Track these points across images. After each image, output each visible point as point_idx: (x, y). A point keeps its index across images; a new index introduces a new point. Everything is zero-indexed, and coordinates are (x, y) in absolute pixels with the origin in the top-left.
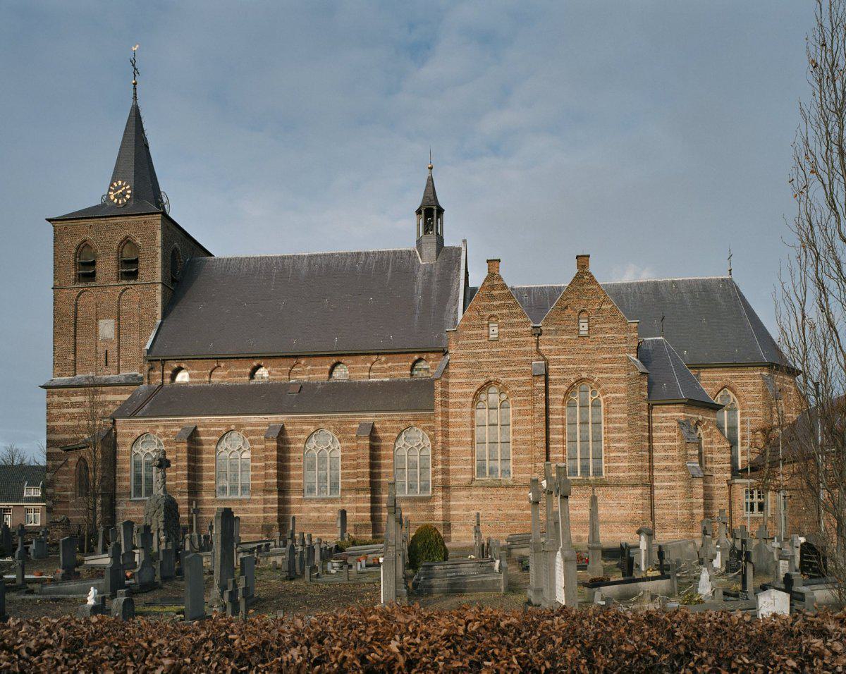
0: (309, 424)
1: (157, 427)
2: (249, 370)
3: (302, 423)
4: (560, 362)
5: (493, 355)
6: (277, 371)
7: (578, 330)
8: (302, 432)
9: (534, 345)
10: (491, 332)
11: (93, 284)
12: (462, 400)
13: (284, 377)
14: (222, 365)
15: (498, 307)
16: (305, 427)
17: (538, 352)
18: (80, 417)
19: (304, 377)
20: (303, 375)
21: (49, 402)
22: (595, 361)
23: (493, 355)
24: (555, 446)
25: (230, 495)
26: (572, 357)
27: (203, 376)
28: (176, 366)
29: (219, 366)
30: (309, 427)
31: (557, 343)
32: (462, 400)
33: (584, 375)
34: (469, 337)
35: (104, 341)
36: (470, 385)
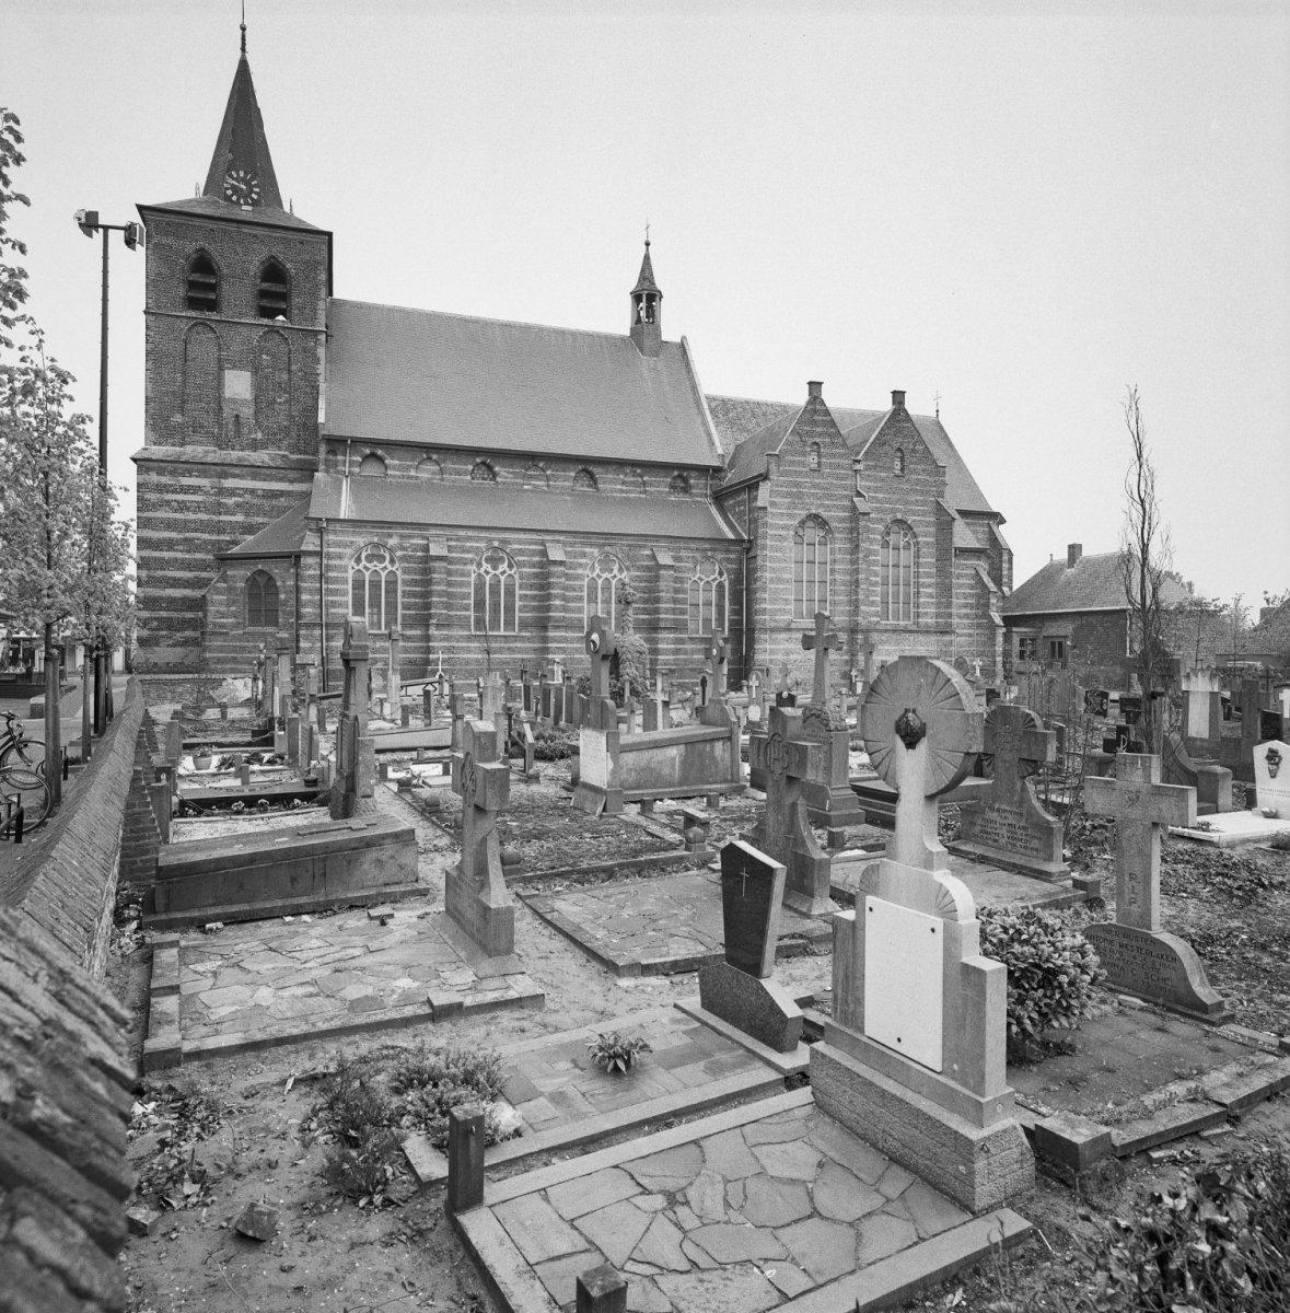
0: (591, 545)
1: (390, 536)
5: (815, 486)
8: (584, 555)
12: (783, 533)
14: (435, 457)
15: (820, 435)
16: (587, 550)
18: (198, 508)
21: (142, 481)
22: (907, 503)
23: (815, 486)
25: (520, 631)
27: (408, 468)
28: (368, 451)
31: (876, 479)
32: (783, 533)
33: (899, 516)
34: (792, 463)
35: (234, 401)
36: (791, 516)
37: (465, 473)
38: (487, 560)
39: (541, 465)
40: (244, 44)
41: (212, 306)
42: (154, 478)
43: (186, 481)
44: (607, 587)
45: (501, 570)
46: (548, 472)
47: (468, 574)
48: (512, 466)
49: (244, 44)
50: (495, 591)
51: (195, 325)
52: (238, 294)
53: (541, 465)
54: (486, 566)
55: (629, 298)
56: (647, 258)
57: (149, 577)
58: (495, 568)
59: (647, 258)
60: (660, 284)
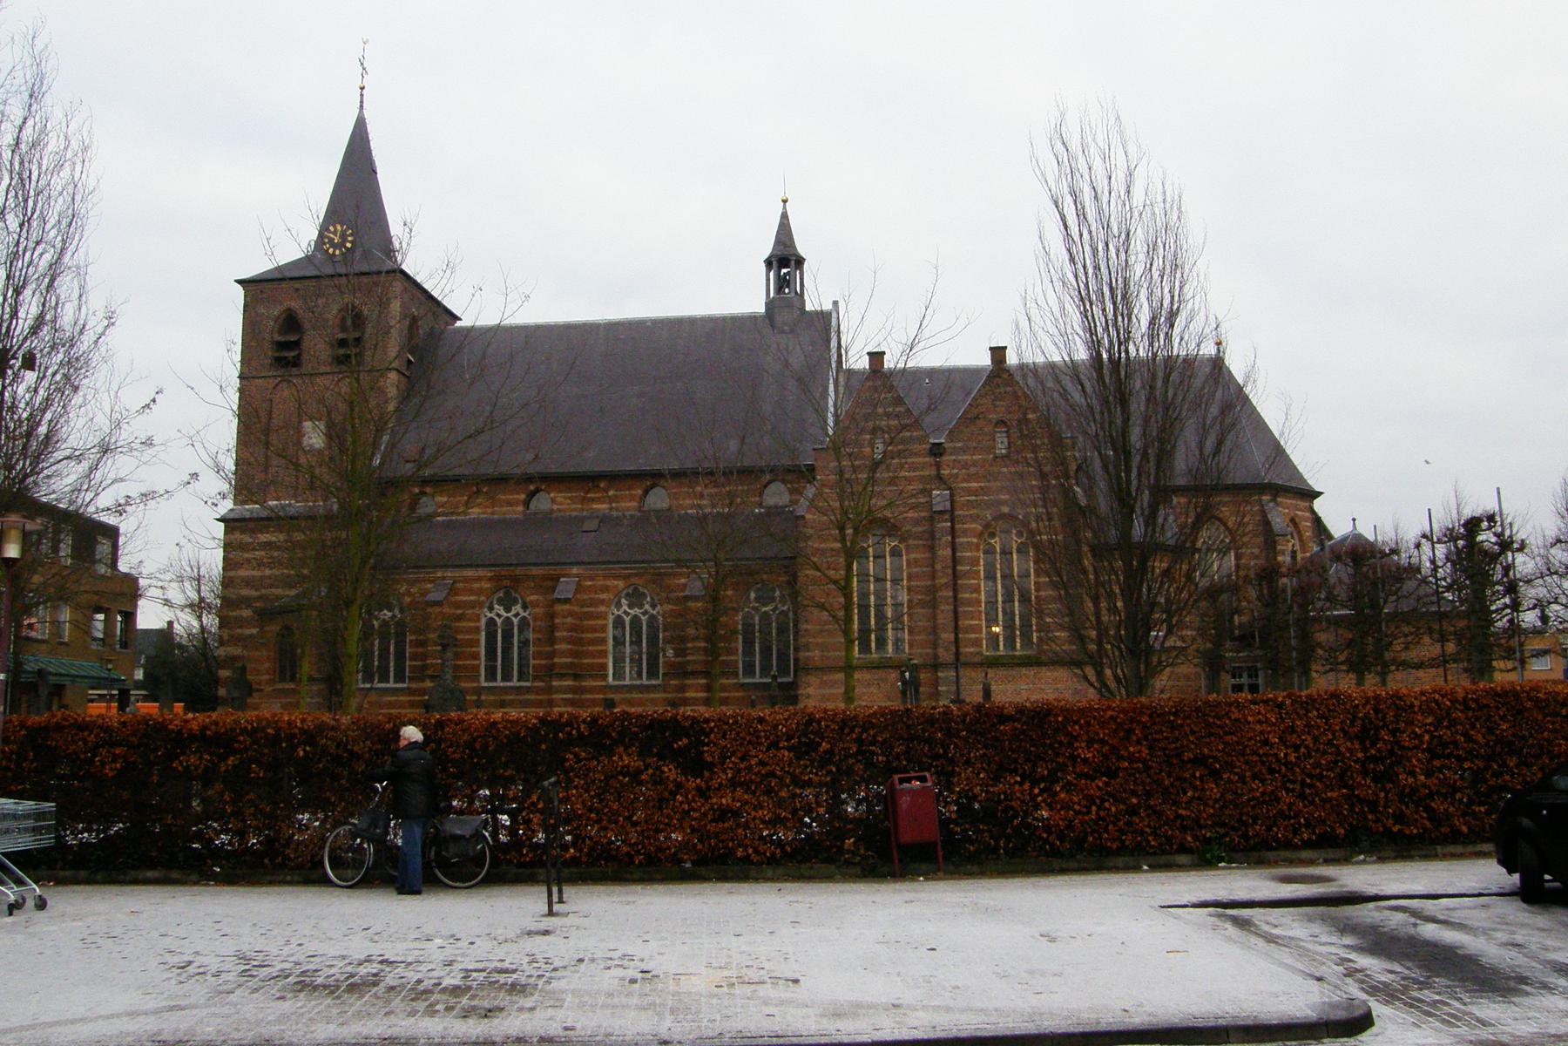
0: (617, 577)
2: (523, 497)
3: (606, 577)
4: (969, 491)
6: (564, 497)
7: (994, 448)
8: (606, 589)
9: (934, 468)
10: (876, 451)
11: (295, 371)
13: (574, 506)
16: (609, 583)
17: (939, 478)
19: (604, 506)
20: (602, 503)
24: (966, 609)
26: (987, 484)
29: (479, 491)
30: (616, 583)
33: (1006, 510)
37: (517, 504)
38: (500, 602)
39: (602, 485)
40: (362, 102)
41: (296, 362)
42: (238, 536)
43: (263, 538)
44: (636, 621)
45: (513, 612)
46: (611, 493)
47: (603, 616)
48: (570, 490)
49: (362, 102)
50: (508, 635)
51: (280, 382)
52: (317, 346)
53: (602, 485)
54: (499, 609)
55: (764, 265)
56: (784, 216)
57: (231, 636)
58: (508, 610)
59: (784, 216)
60: (802, 248)
